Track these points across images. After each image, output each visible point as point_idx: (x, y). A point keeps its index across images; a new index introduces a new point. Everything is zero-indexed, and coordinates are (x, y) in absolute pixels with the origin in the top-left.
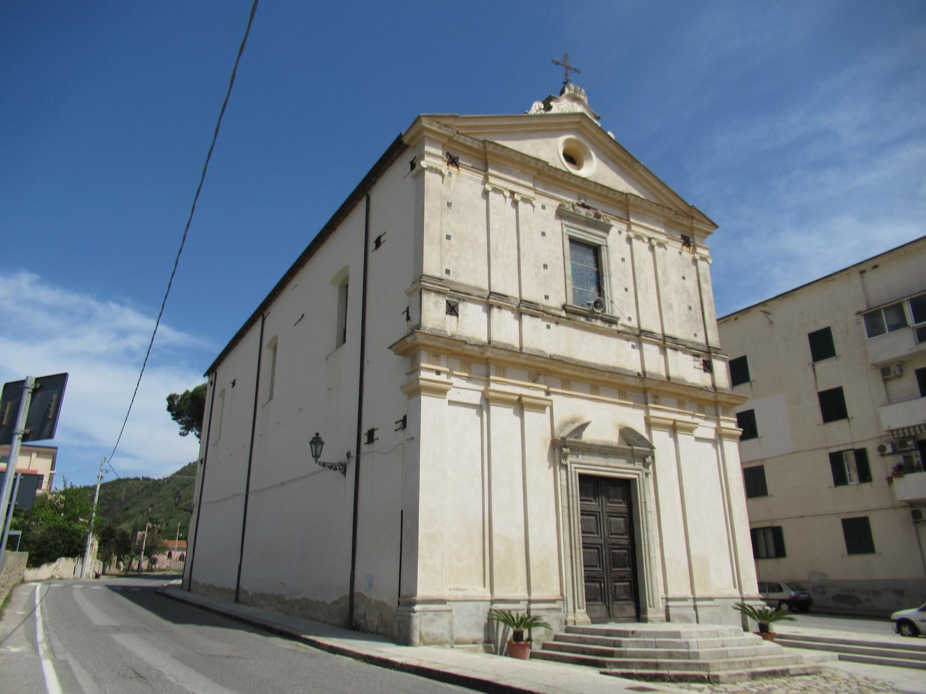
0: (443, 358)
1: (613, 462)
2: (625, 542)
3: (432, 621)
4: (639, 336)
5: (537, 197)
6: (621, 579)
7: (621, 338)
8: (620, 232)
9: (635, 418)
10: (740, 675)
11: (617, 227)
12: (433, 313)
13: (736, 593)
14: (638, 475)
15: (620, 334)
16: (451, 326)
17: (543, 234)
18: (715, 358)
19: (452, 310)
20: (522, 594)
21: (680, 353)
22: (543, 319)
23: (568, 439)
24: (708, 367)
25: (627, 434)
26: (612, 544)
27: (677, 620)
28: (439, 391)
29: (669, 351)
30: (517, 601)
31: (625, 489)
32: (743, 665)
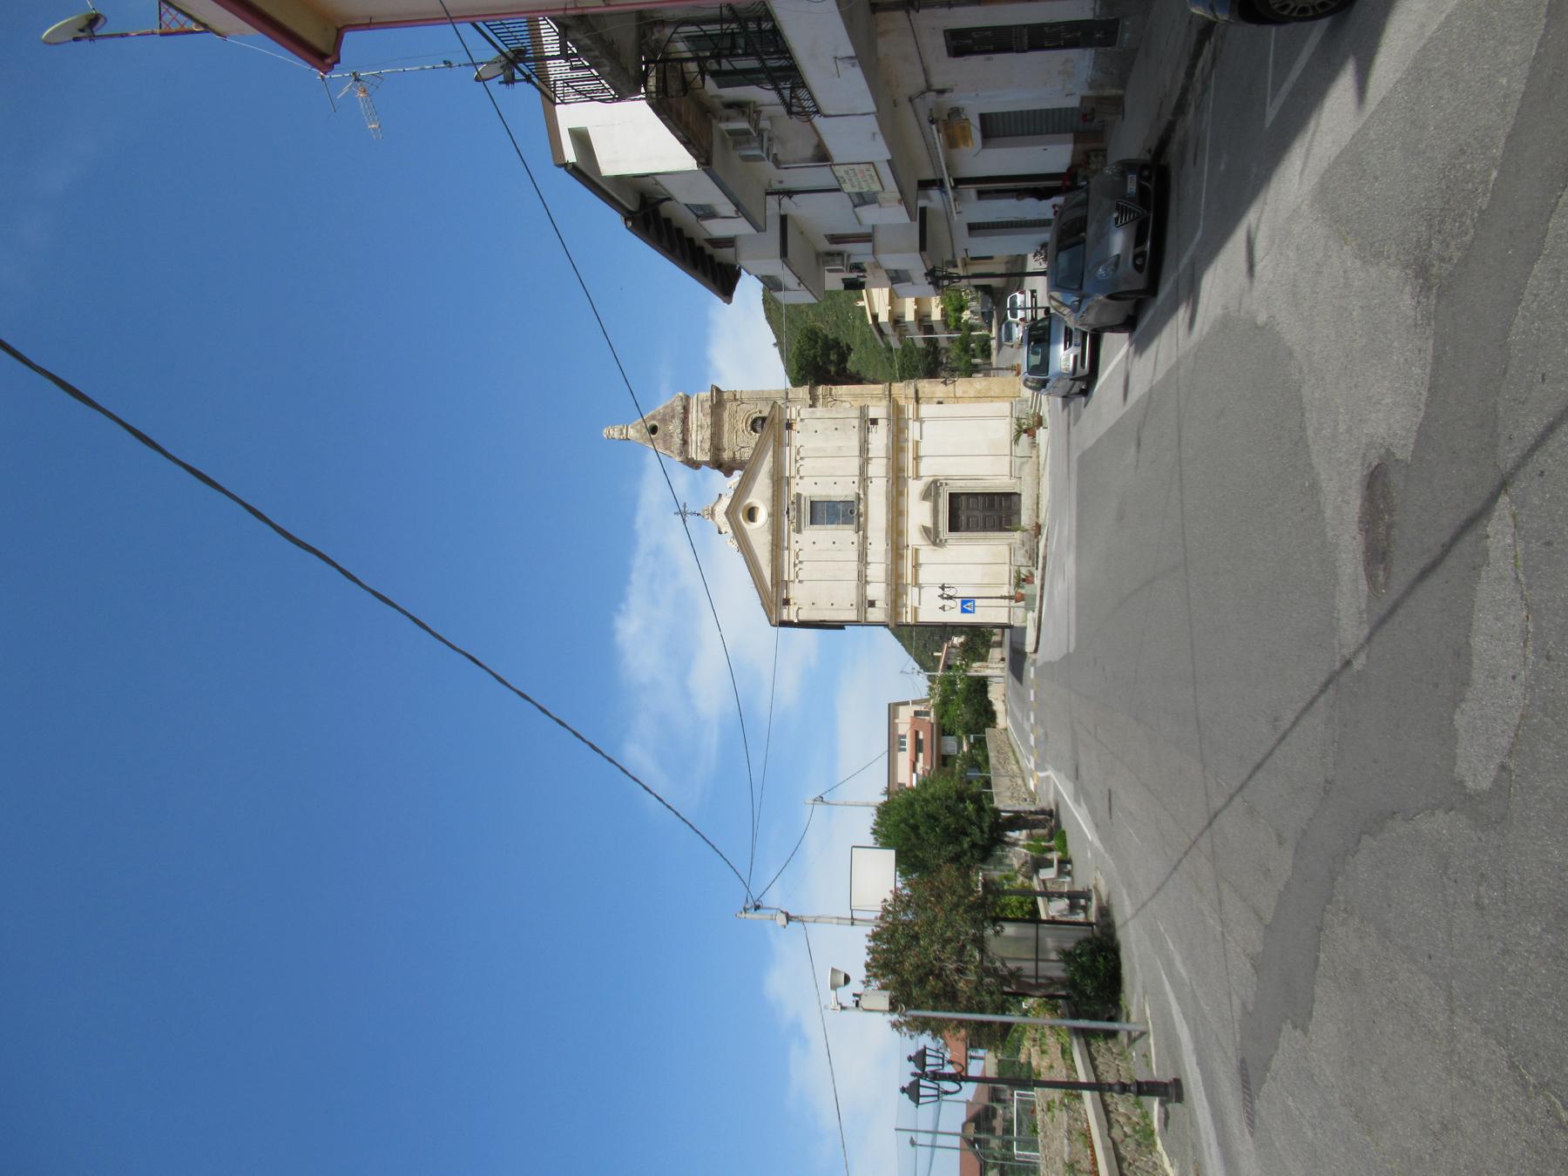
4: (864, 479)
9: (915, 489)
12: (876, 614)
15: (865, 494)
16: (880, 604)
19: (872, 604)
20: (1006, 567)
24: (874, 422)
25: (926, 496)
31: (954, 497)
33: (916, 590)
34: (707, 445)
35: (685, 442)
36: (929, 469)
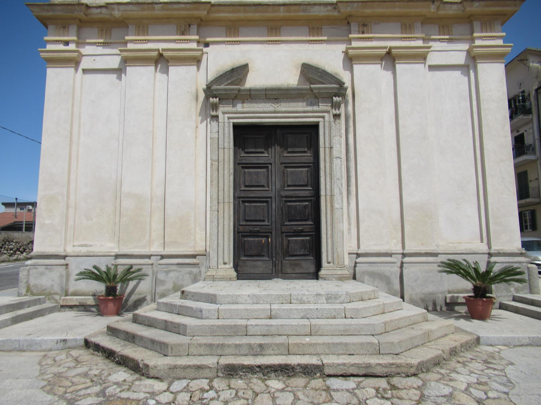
0: (73, 29)
1: (283, 107)
2: (307, 193)
3: (42, 274)
6: (298, 233)
10: (199, 367)
13: (483, 248)
14: (323, 117)
20: (156, 248)
23: (214, 87)
26: (286, 197)
27: (366, 278)
28: (74, 62)
30: (149, 257)
31: (307, 135)
32: (244, 351)
33: (114, 62)
36: (369, 82)
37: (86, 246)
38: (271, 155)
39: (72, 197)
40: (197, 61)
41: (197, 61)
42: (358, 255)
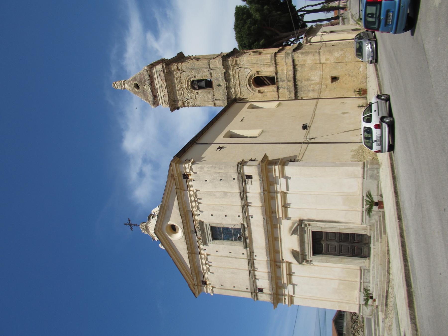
0: (280, 297)
3: (365, 311)
5: (203, 253)
7: (250, 224)
8: (199, 215)
9: (285, 227)
11: (198, 218)
15: (249, 225)
17: (217, 251)
18: (243, 173)
19: (261, 290)
20: (358, 280)
21: (248, 194)
22: (254, 259)
24: (249, 177)
29: (249, 201)
34: (167, 98)
35: (155, 96)
36: (295, 214)
37: (356, 298)
38: (324, 243)
39: (339, 301)
40: (289, 264)
41: (289, 264)
42: (363, 222)
